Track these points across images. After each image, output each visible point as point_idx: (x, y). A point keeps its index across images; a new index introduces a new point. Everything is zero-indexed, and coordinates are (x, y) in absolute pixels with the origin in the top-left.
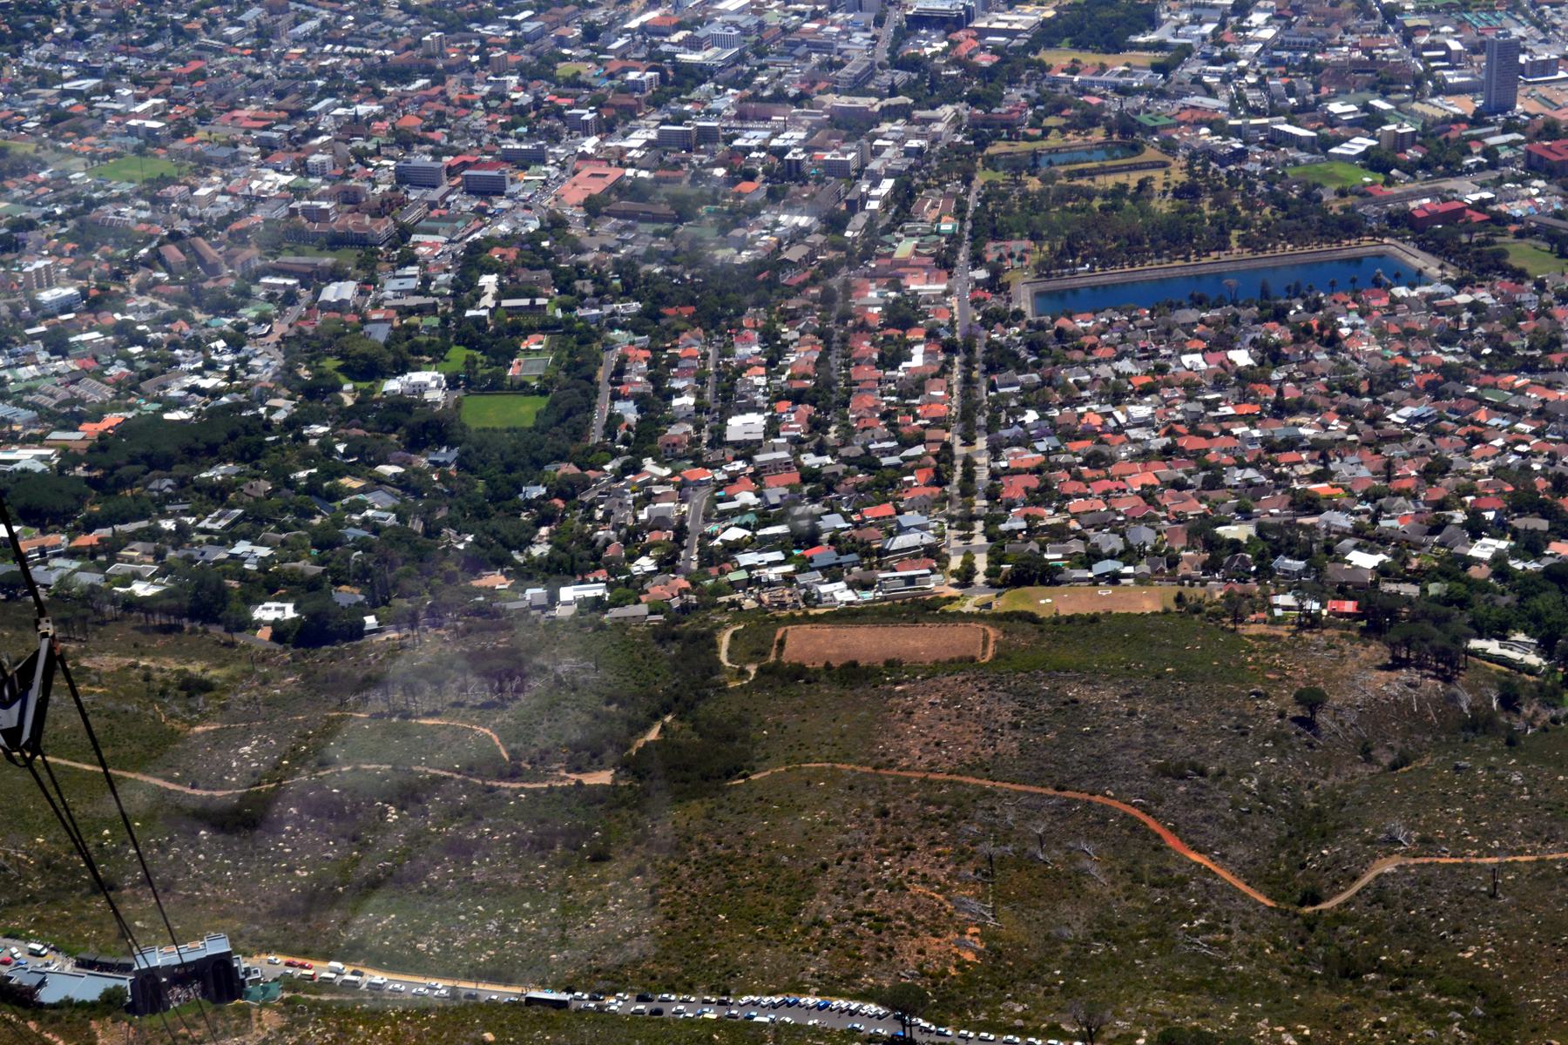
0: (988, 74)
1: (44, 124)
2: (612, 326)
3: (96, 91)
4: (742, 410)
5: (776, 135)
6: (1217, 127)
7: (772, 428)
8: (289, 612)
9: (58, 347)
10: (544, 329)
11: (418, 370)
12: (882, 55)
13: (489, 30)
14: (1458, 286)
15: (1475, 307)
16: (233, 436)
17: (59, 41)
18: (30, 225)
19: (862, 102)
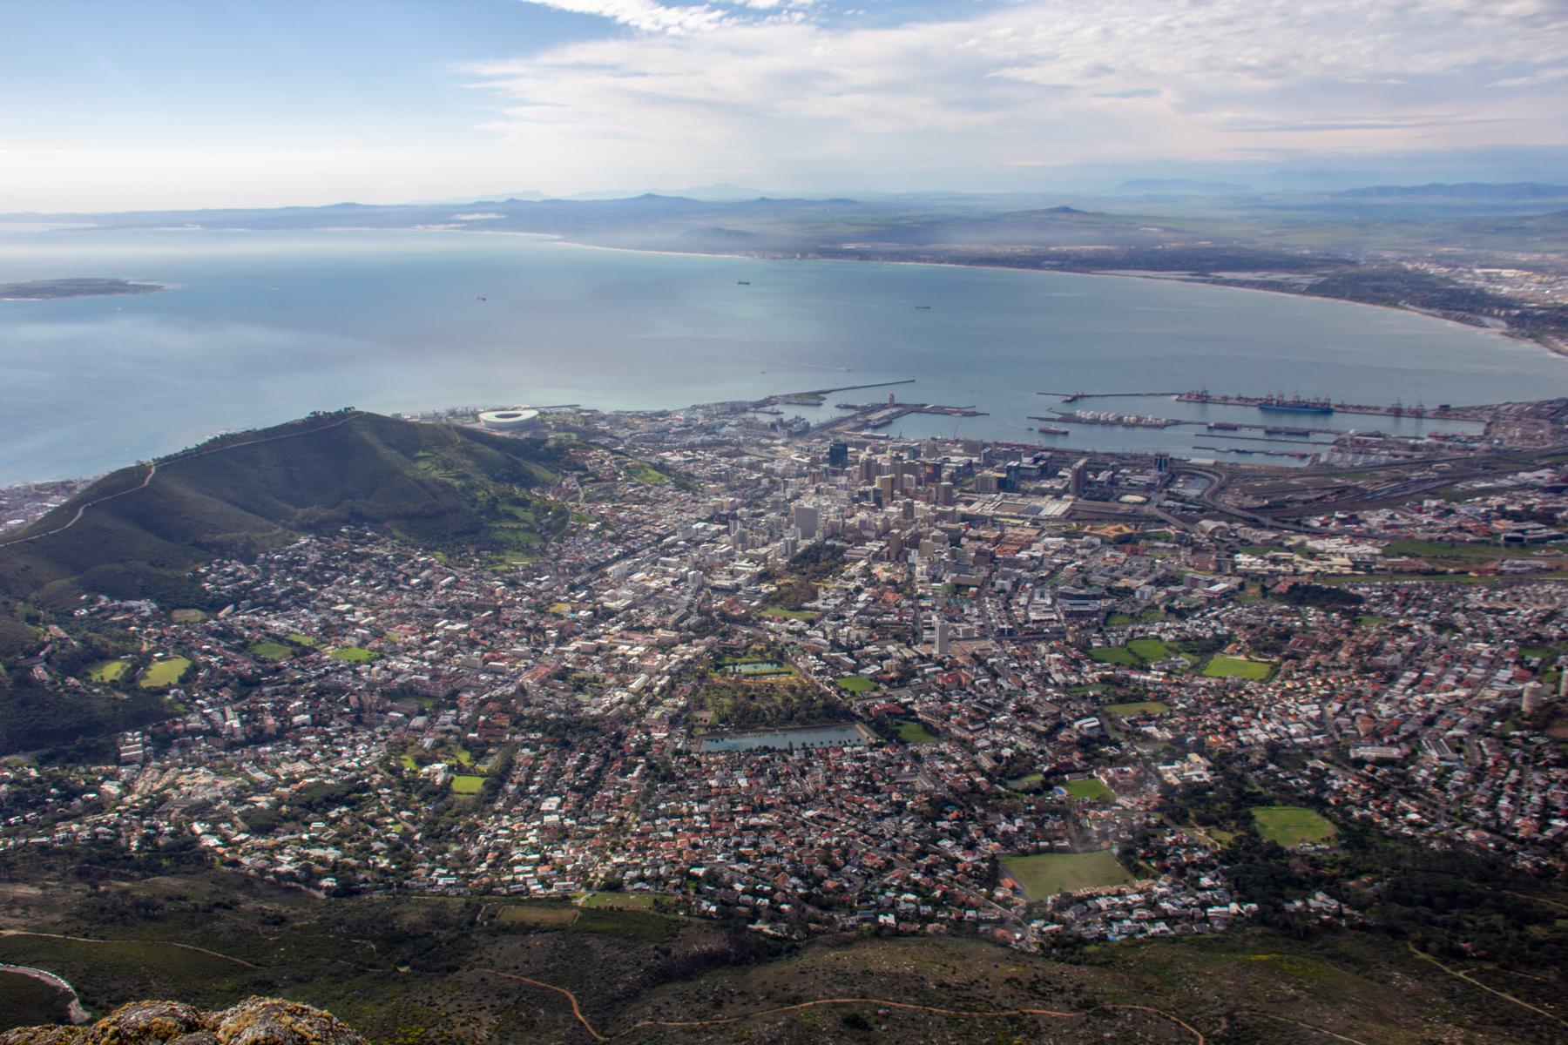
0: (735, 620)
1: (321, 629)
2: (526, 746)
3: (348, 611)
4: (556, 794)
5: (632, 647)
6: (818, 655)
7: (560, 806)
9: (297, 743)
10: (500, 744)
11: (439, 762)
12: (694, 610)
13: (529, 585)
14: (872, 747)
15: (874, 759)
16: (349, 793)
17: (340, 584)
18: (301, 682)
19: (673, 634)
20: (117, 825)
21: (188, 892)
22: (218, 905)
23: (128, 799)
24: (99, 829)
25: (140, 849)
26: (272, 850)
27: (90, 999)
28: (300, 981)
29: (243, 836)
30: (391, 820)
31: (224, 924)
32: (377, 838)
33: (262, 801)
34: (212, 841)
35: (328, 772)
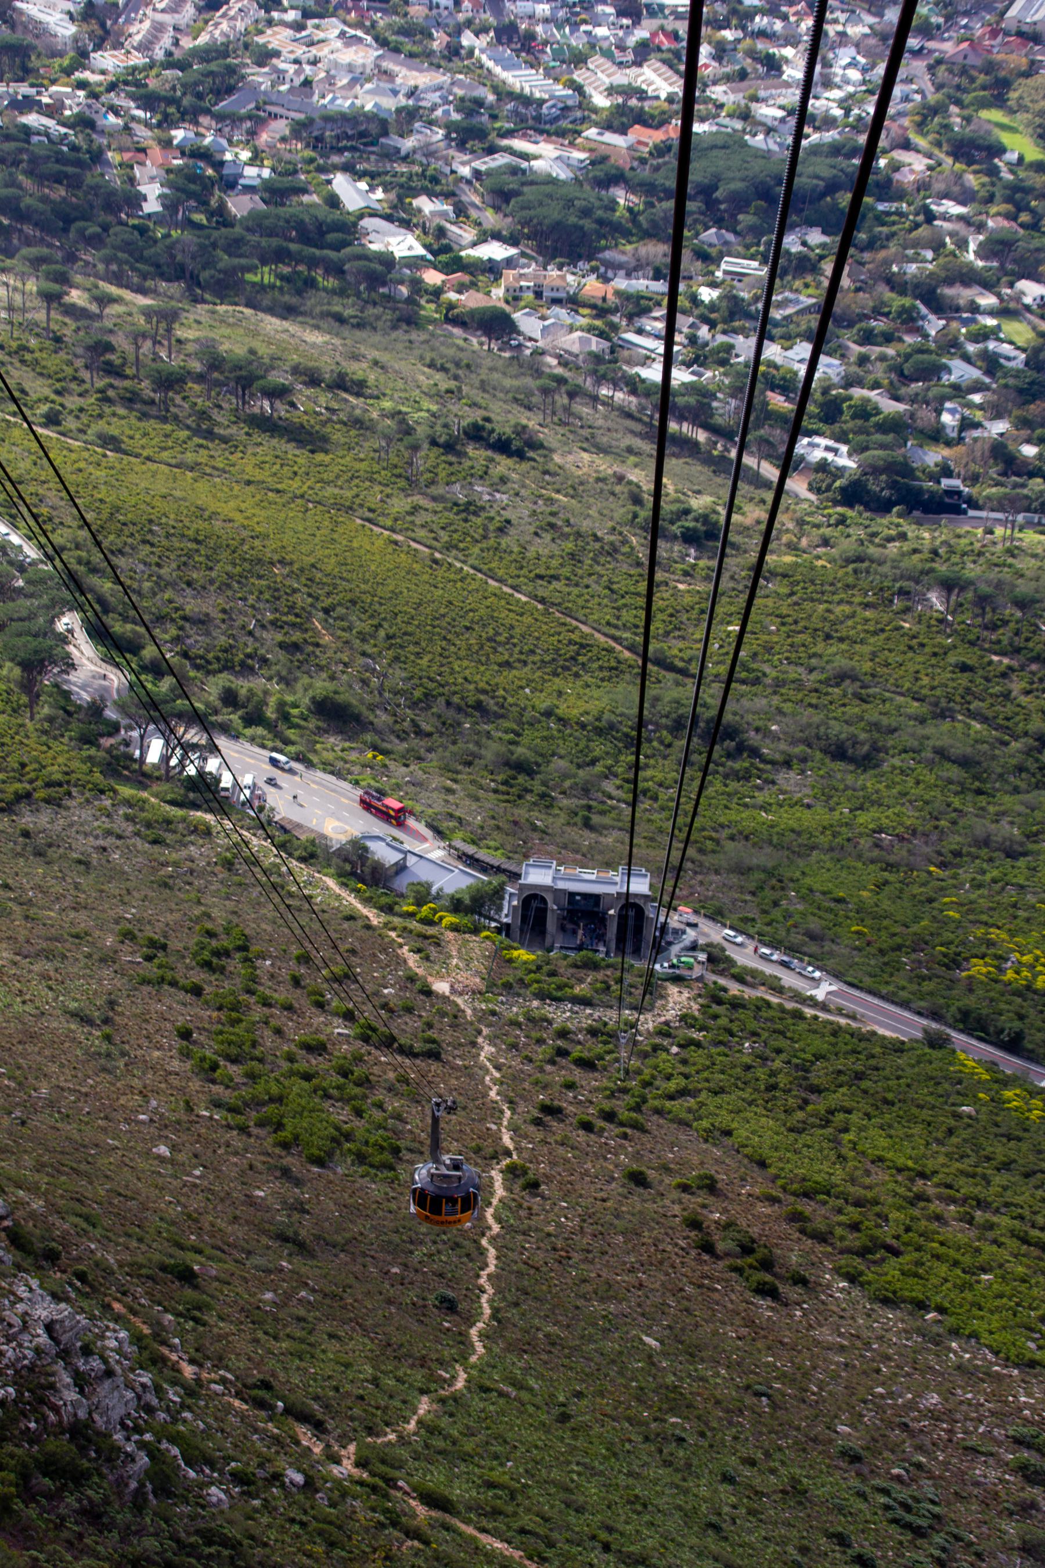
8: (845, 460)
20: (84, 123)
21: (357, 370)
22: (476, 434)
23: (108, 61)
24: (32, 119)
25: (170, 205)
26: (601, 311)
27: (118, 627)
28: (839, 752)
29: (496, 251)
30: (987, 300)
31: (509, 494)
32: (951, 345)
33: (547, 157)
34: (404, 245)
35: (745, 116)
